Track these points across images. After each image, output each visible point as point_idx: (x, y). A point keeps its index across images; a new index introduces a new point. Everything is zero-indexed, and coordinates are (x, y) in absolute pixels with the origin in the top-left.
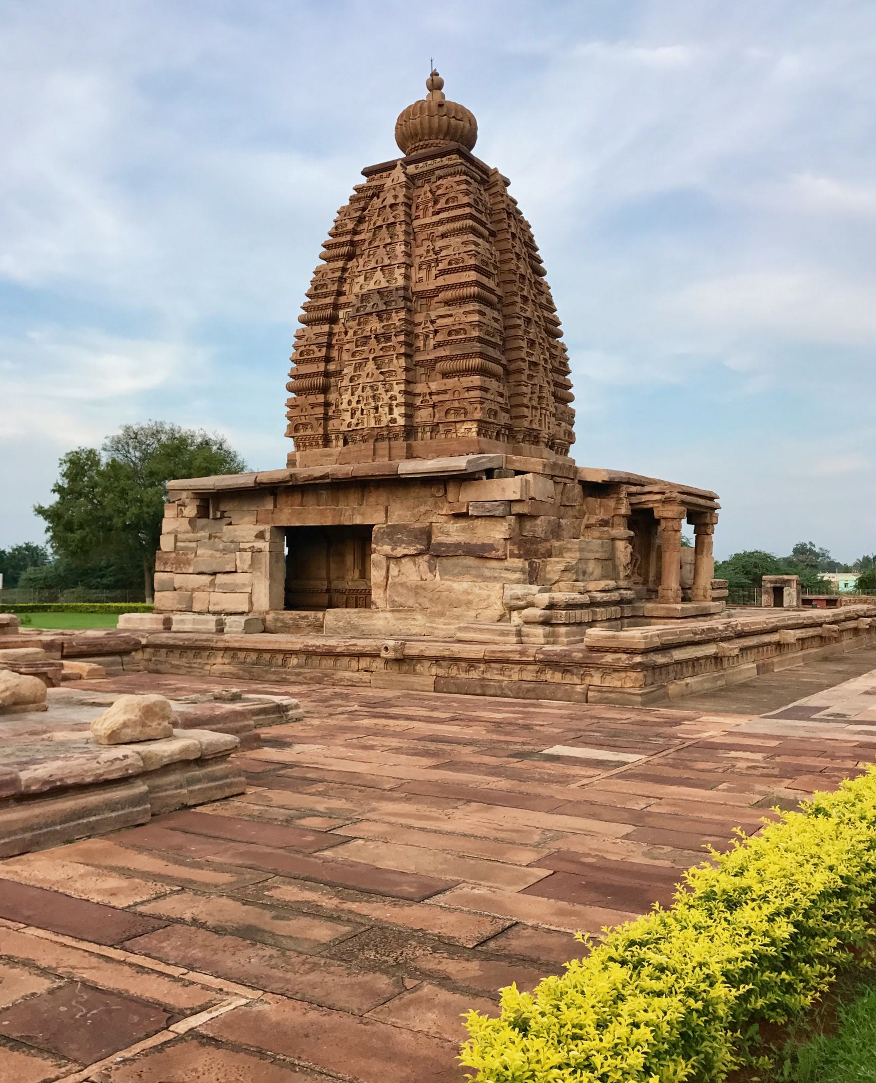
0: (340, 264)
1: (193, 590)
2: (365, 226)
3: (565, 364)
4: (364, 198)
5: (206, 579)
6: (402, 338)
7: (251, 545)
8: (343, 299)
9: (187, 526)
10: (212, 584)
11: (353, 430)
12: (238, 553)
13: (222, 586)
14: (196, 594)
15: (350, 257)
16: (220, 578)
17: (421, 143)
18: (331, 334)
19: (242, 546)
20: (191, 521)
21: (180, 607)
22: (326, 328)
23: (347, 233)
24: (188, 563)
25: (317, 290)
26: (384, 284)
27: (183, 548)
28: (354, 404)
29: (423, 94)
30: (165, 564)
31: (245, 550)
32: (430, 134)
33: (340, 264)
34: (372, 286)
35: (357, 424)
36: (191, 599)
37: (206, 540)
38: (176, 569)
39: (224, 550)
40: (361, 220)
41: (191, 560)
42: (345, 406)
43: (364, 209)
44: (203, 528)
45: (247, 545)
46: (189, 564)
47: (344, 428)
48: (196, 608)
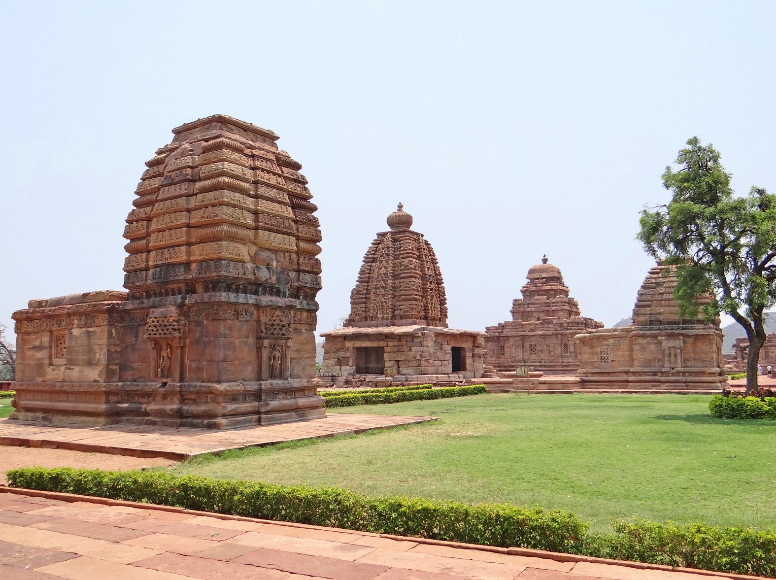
0: (370, 264)
2: (377, 253)
3: (444, 293)
4: (377, 243)
6: (391, 288)
8: (371, 275)
15: (372, 262)
18: (368, 286)
22: (366, 284)
23: (371, 254)
25: (362, 272)
28: (375, 308)
29: (396, 209)
33: (370, 264)
40: (376, 251)
42: (371, 308)
43: (377, 247)
47: (371, 315)
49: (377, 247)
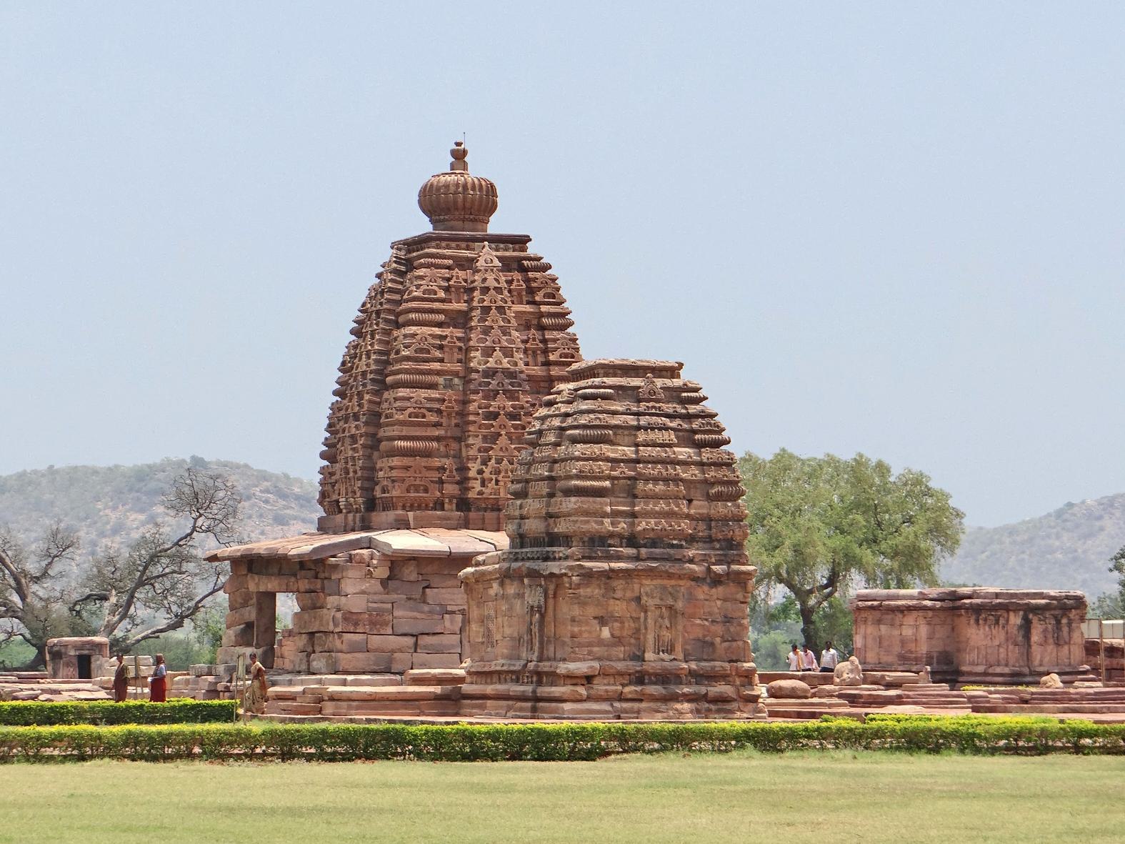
1: (393, 651)
5: (409, 641)
7: (461, 608)
9: (379, 588)
10: (416, 645)
11: (485, 498)
12: (447, 616)
13: (425, 647)
14: (396, 655)
16: (425, 640)
17: (471, 217)
19: (449, 608)
20: (384, 583)
21: (376, 668)
24: (385, 624)
26: (505, 362)
27: (374, 610)
28: (487, 475)
30: (356, 624)
31: (453, 612)
32: (479, 210)
34: (492, 363)
35: (491, 494)
36: (391, 660)
37: (403, 602)
38: (370, 630)
39: (430, 612)
41: (389, 621)
44: (395, 591)
45: (455, 608)
46: (387, 625)
48: (395, 668)
49: (448, 280)
